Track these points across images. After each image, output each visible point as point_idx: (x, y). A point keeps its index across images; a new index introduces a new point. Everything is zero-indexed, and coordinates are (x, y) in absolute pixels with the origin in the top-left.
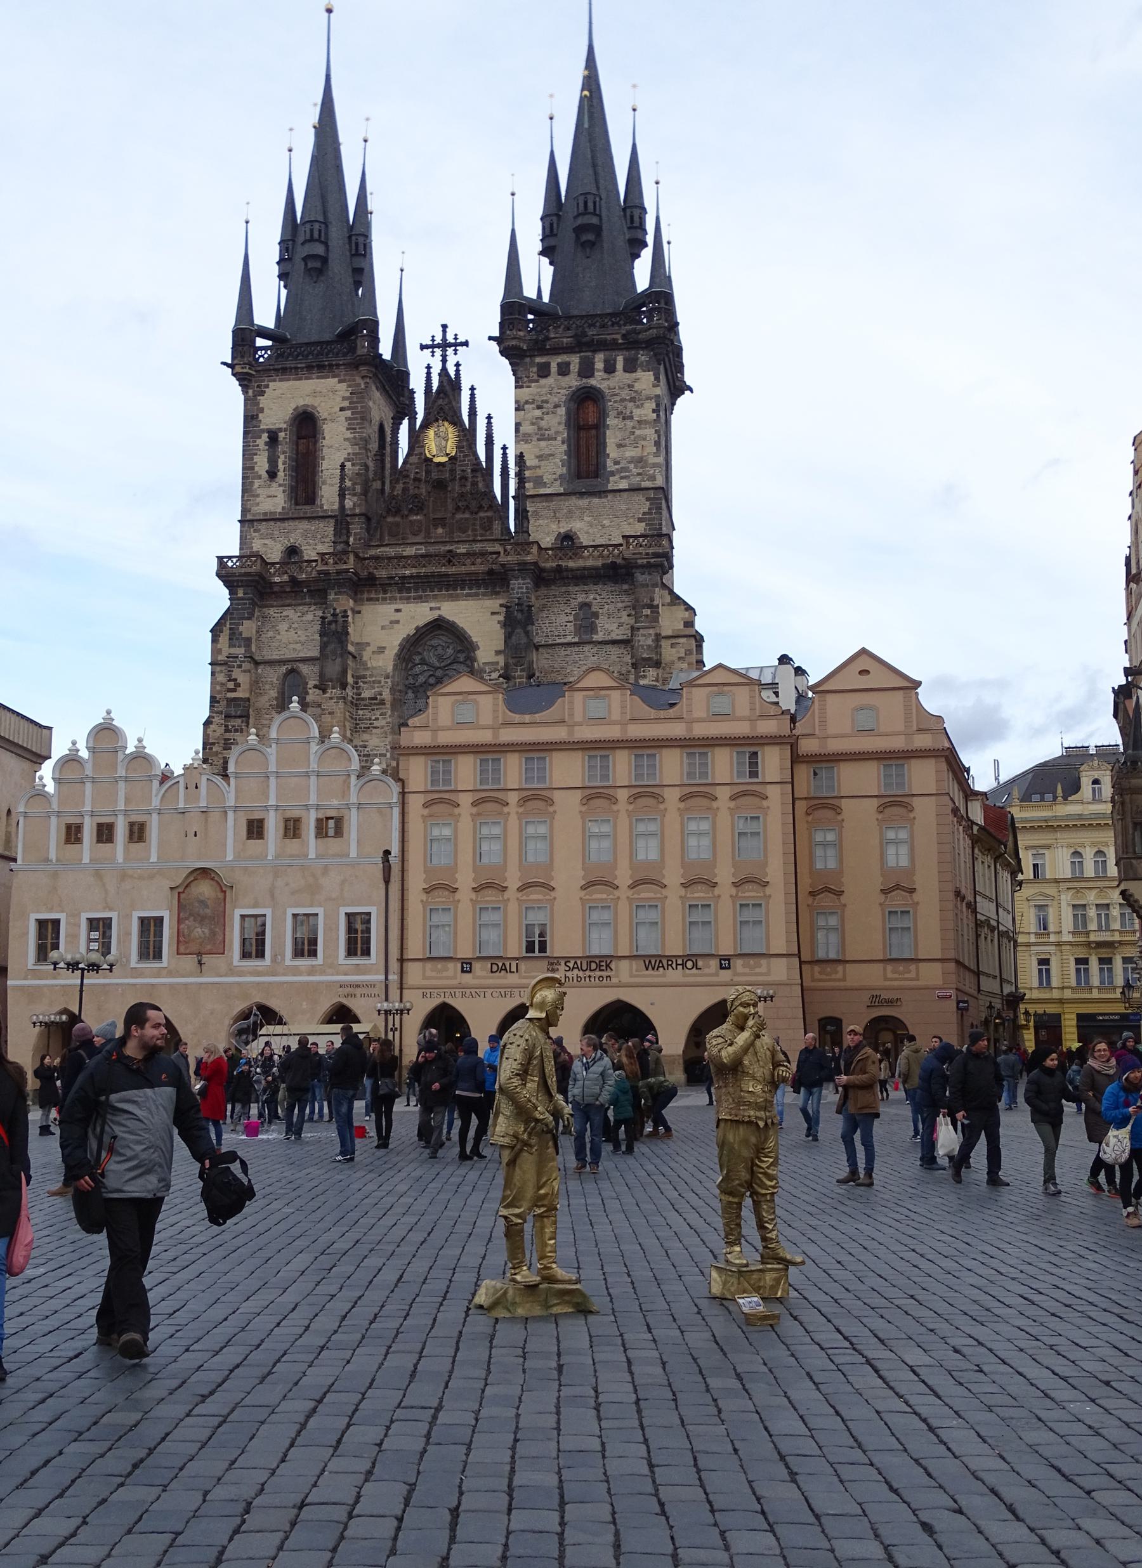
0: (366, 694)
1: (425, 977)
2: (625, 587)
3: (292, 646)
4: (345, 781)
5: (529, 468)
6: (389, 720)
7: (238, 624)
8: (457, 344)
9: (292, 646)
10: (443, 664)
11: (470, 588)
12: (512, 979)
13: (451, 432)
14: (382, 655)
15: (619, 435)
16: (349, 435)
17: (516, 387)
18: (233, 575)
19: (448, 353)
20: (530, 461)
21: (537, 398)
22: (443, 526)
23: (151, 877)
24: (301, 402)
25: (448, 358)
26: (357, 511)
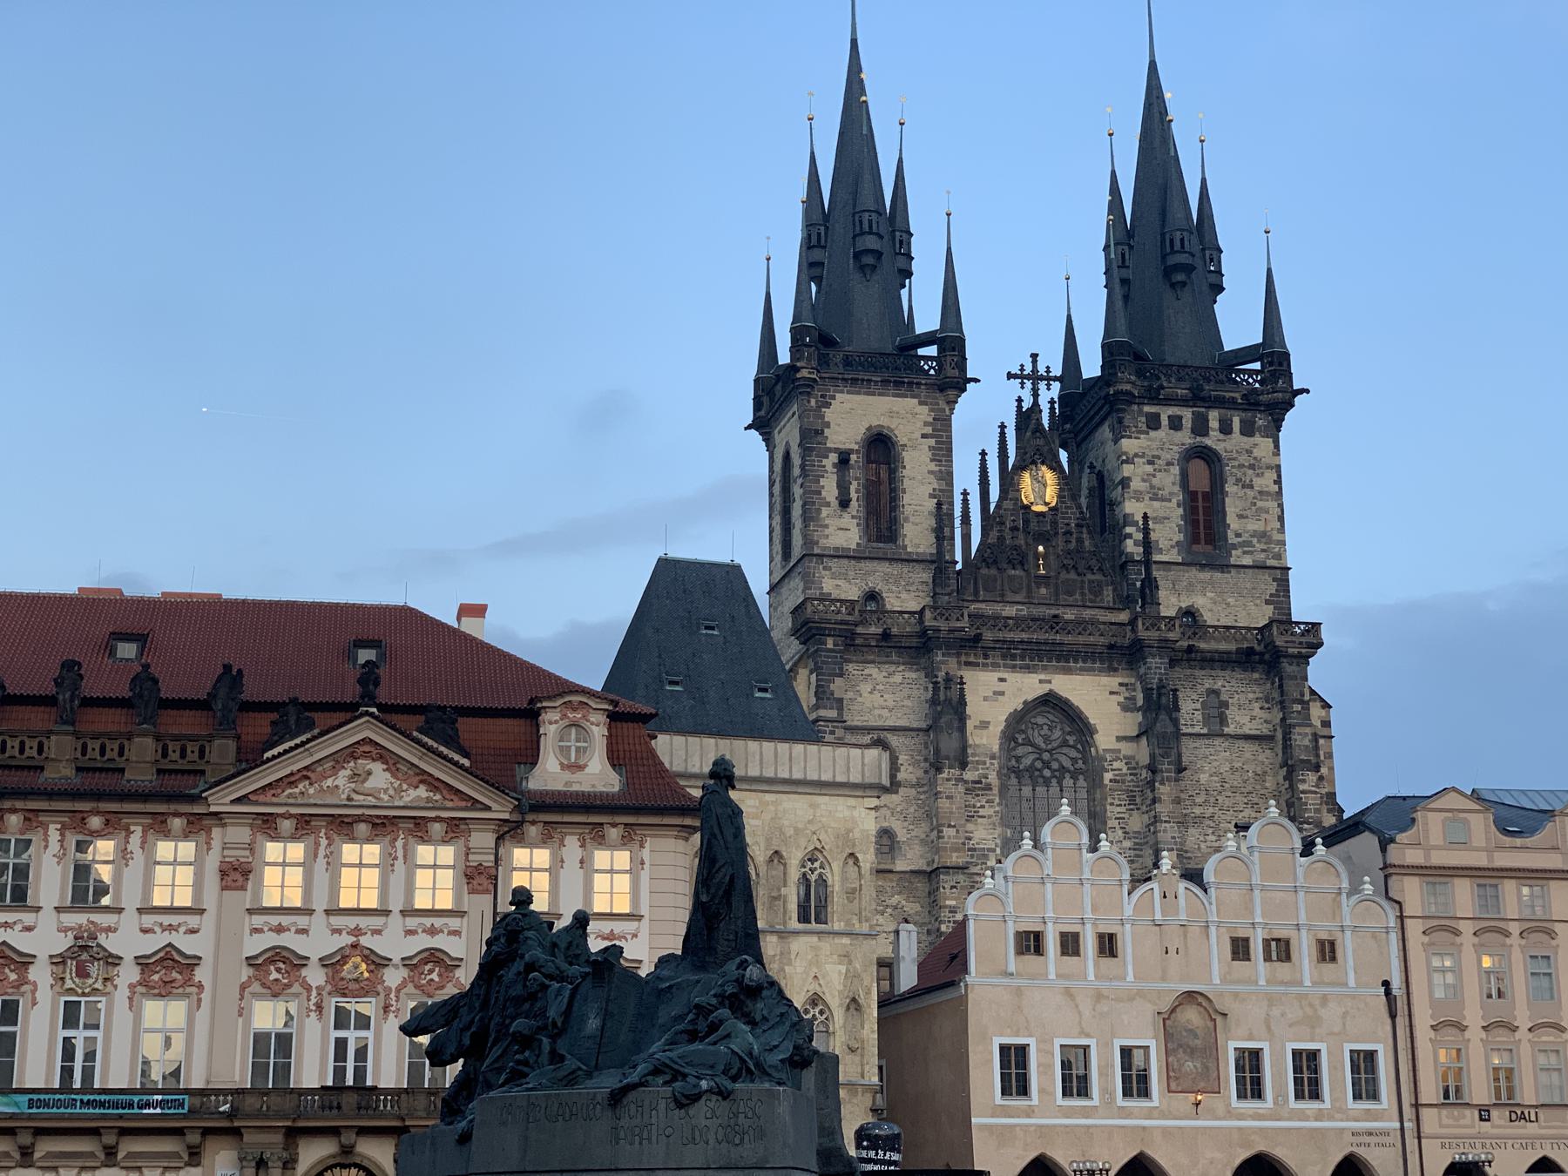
1: (1441, 1126)
3: (877, 712)
4: (1334, 900)
6: (997, 809)
7: (830, 681)
9: (877, 712)
10: (1050, 747)
11: (1084, 662)
12: (1532, 1129)
13: (1049, 476)
14: (985, 732)
15: (1240, 504)
16: (933, 467)
21: (1147, 451)
22: (1047, 586)
23: (1131, 999)
24: (875, 423)
25: (1040, 392)
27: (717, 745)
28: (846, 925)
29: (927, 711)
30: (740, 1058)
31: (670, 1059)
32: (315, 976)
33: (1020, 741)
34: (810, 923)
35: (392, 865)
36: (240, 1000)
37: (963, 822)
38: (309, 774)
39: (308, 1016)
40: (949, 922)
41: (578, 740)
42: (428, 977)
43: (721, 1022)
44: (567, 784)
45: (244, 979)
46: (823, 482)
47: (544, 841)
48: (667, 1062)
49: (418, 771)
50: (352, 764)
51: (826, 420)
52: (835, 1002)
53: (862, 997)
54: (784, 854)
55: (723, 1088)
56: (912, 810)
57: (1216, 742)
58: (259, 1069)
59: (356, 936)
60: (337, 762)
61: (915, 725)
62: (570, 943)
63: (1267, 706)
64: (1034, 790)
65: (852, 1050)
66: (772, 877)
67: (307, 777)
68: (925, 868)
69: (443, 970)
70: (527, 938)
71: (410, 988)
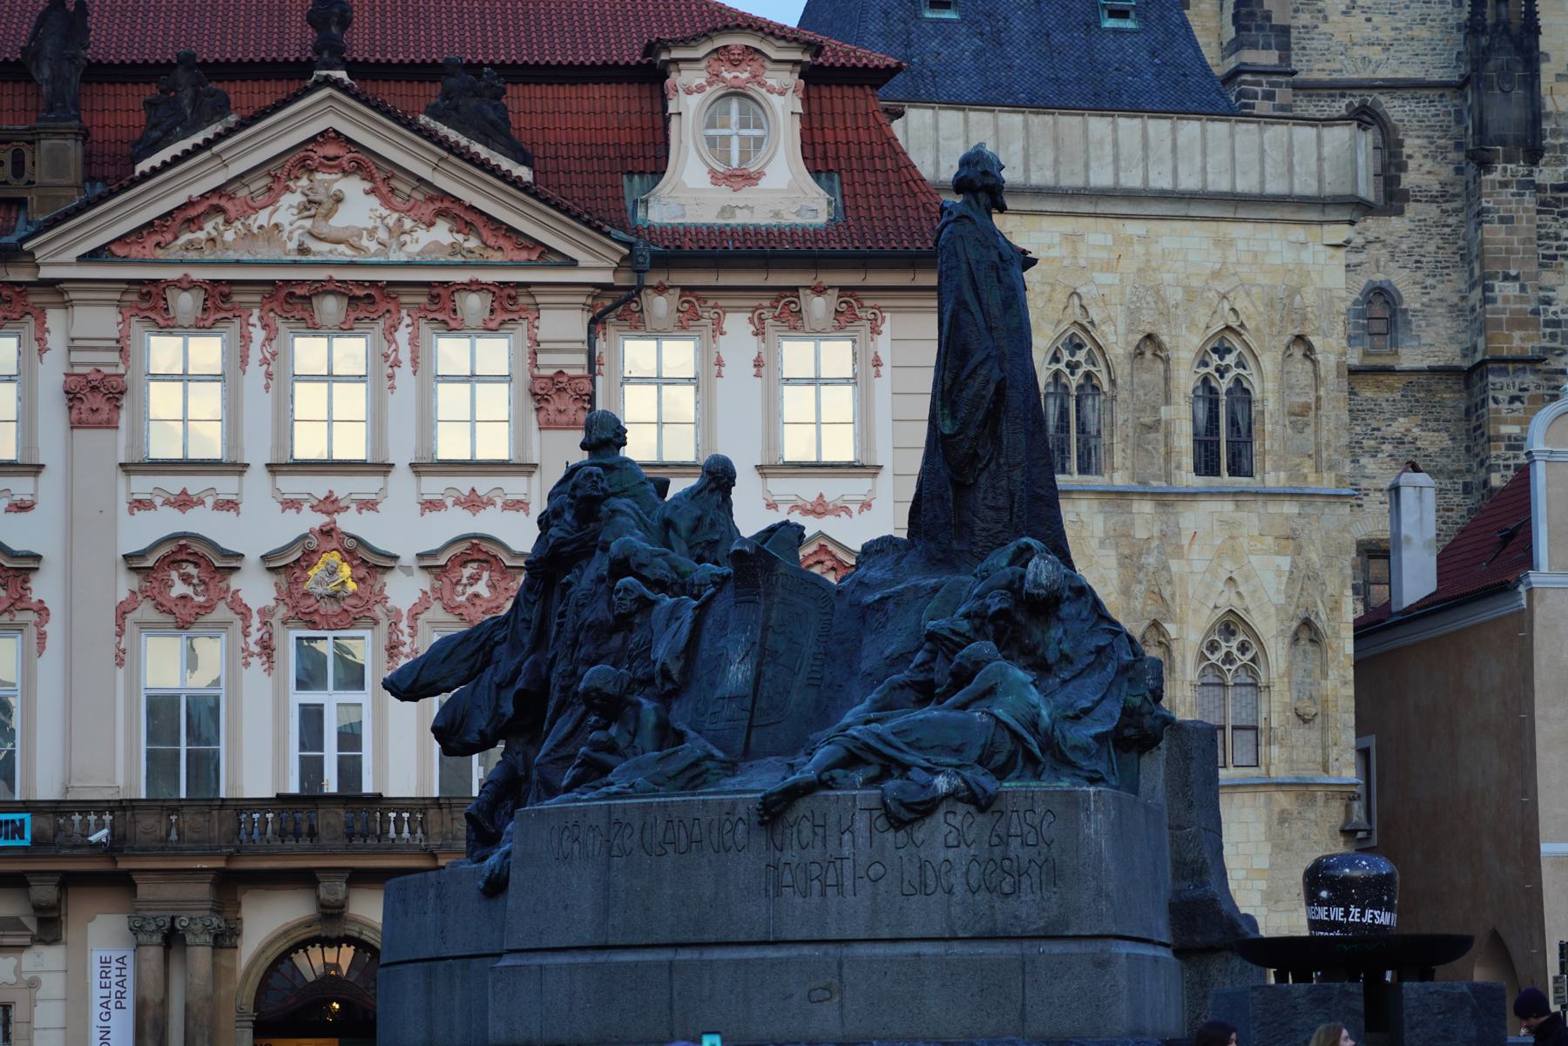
3: (1358, 52)
9: (1358, 52)
27: (1026, 126)
28: (1289, 478)
29: (1462, 48)
30: (1015, 735)
31: (879, 737)
32: (256, 589)
34: (1218, 474)
35: (391, 377)
36: (119, 635)
37: (1535, 268)
38: (223, 202)
39: (247, 664)
40: (1507, 467)
41: (744, 124)
42: (470, 590)
43: (978, 665)
44: (726, 210)
45: (123, 595)
47: (684, 324)
48: (872, 742)
49: (431, 192)
50: (304, 182)
52: (1270, 627)
53: (1323, 617)
54: (1165, 339)
55: (978, 790)
56: (1431, 247)
58: (160, 765)
59: (329, 513)
60: (276, 178)
61: (1436, 76)
62: (699, 519)
65: (1304, 719)
66: (1143, 386)
67: (219, 210)
68: (1458, 362)
69: (497, 576)
70: (614, 512)
71: (437, 612)
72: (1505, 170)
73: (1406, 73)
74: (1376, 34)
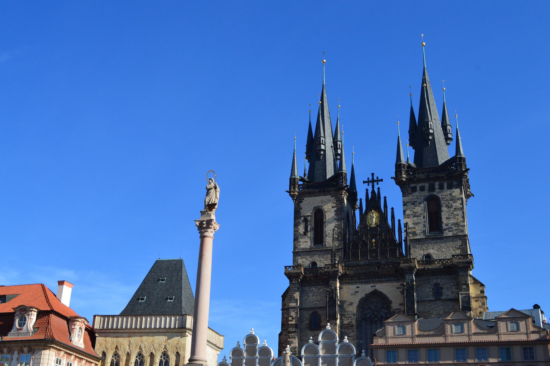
0: (346, 322)
2: (454, 276)
3: (314, 302)
5: (409, 228)
6: (355, 333)
8: (379, 180)
10: (377, 309)
17: (403, 196)
18: (291, 273)
19: (374, 184)
20: (410, 225)
24: (317, 205)
26: (340, 247)
33: (366, 308)
46: (299, 227)
51: (301, 207)
57: (438, 303)
63: (458, 287)
64: (371, 326)
72: (332, 321)
73: (322, 306)
74: (318, 299)
